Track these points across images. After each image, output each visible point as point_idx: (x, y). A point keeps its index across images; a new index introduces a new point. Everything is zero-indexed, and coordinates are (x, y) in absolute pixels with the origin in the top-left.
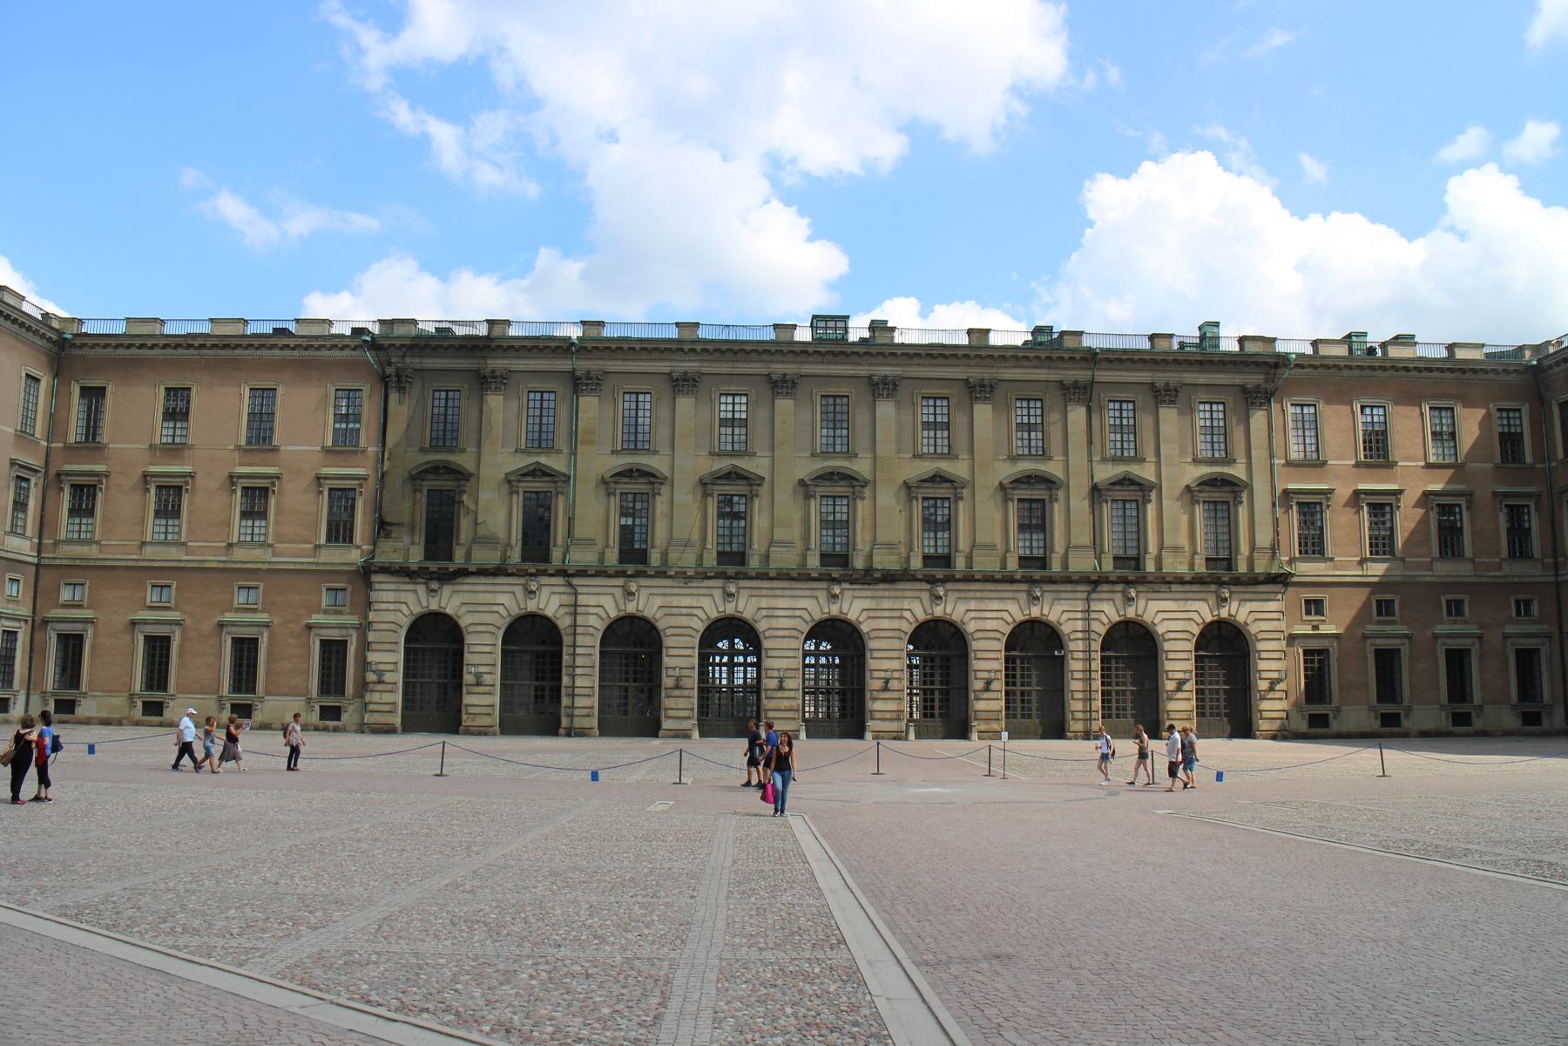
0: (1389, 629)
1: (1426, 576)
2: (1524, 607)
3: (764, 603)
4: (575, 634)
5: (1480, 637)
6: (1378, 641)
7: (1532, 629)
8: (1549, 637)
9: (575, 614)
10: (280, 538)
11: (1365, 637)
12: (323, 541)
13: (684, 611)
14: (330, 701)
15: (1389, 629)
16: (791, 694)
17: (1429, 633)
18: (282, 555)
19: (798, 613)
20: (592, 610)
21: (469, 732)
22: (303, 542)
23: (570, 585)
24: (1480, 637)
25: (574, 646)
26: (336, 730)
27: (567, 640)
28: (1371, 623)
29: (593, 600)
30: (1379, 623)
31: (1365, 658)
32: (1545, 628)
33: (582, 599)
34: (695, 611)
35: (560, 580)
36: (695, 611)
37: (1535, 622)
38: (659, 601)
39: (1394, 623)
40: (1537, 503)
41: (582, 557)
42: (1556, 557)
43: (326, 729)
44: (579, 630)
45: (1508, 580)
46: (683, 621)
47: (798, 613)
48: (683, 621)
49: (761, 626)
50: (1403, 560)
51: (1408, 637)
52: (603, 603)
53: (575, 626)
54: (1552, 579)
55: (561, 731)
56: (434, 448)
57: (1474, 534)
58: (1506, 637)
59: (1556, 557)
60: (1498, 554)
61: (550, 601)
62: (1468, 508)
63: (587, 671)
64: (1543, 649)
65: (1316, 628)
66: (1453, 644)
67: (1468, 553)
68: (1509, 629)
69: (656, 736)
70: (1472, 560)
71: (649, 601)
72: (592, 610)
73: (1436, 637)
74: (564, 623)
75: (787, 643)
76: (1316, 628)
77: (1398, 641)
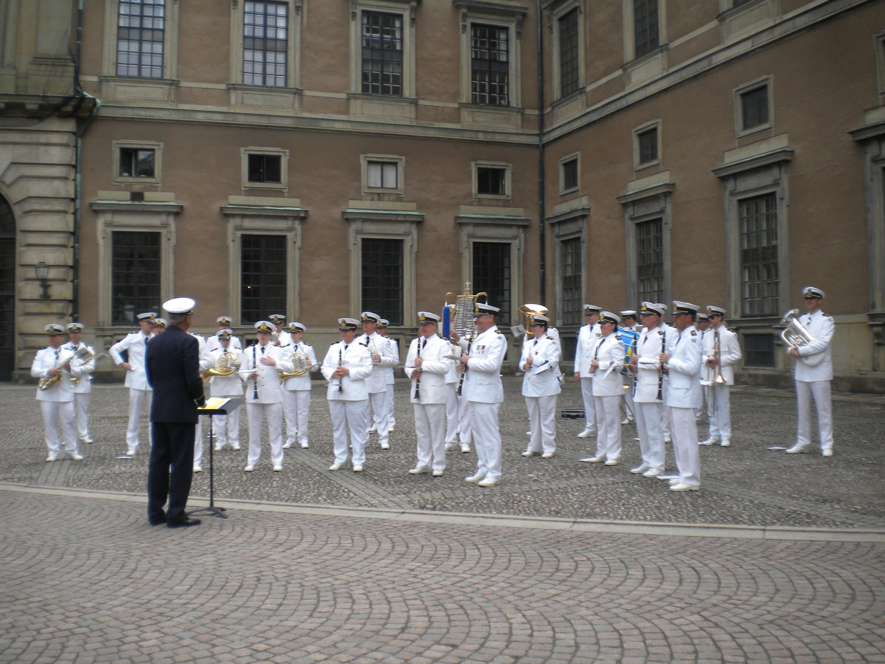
0: (268, 202)
1: (338, 122)
2: (490, 181)
5: (419, 223)
6: (247, 223)
7: (502, 213)
8: (525, 227)
11: (226, 215)
15: (268, 202)
17: (336, 213)
24: (419, 223)
28: (237, 191)
30: (251, 192)
31: (224, 249)
32: (517, 213)
37: (506, 204)
39: (279, 193)
40: (520, 24)
42: (541, 107)
45: (467, 136)
50: (298, 92)
51: (303, 218)
54: (534, 140)
57: (420, 62)
58: (460, 224)
59: (541, 107)
60: (456, 96)
62: (413, 20)
64: (515, 245)
65: (137, 196)
66: (375, 231)
67: (409, 89)
68: (467, 212)
70: (414, 102)
73: (348, 219)
76: (137, 196)
77: (281, 224)
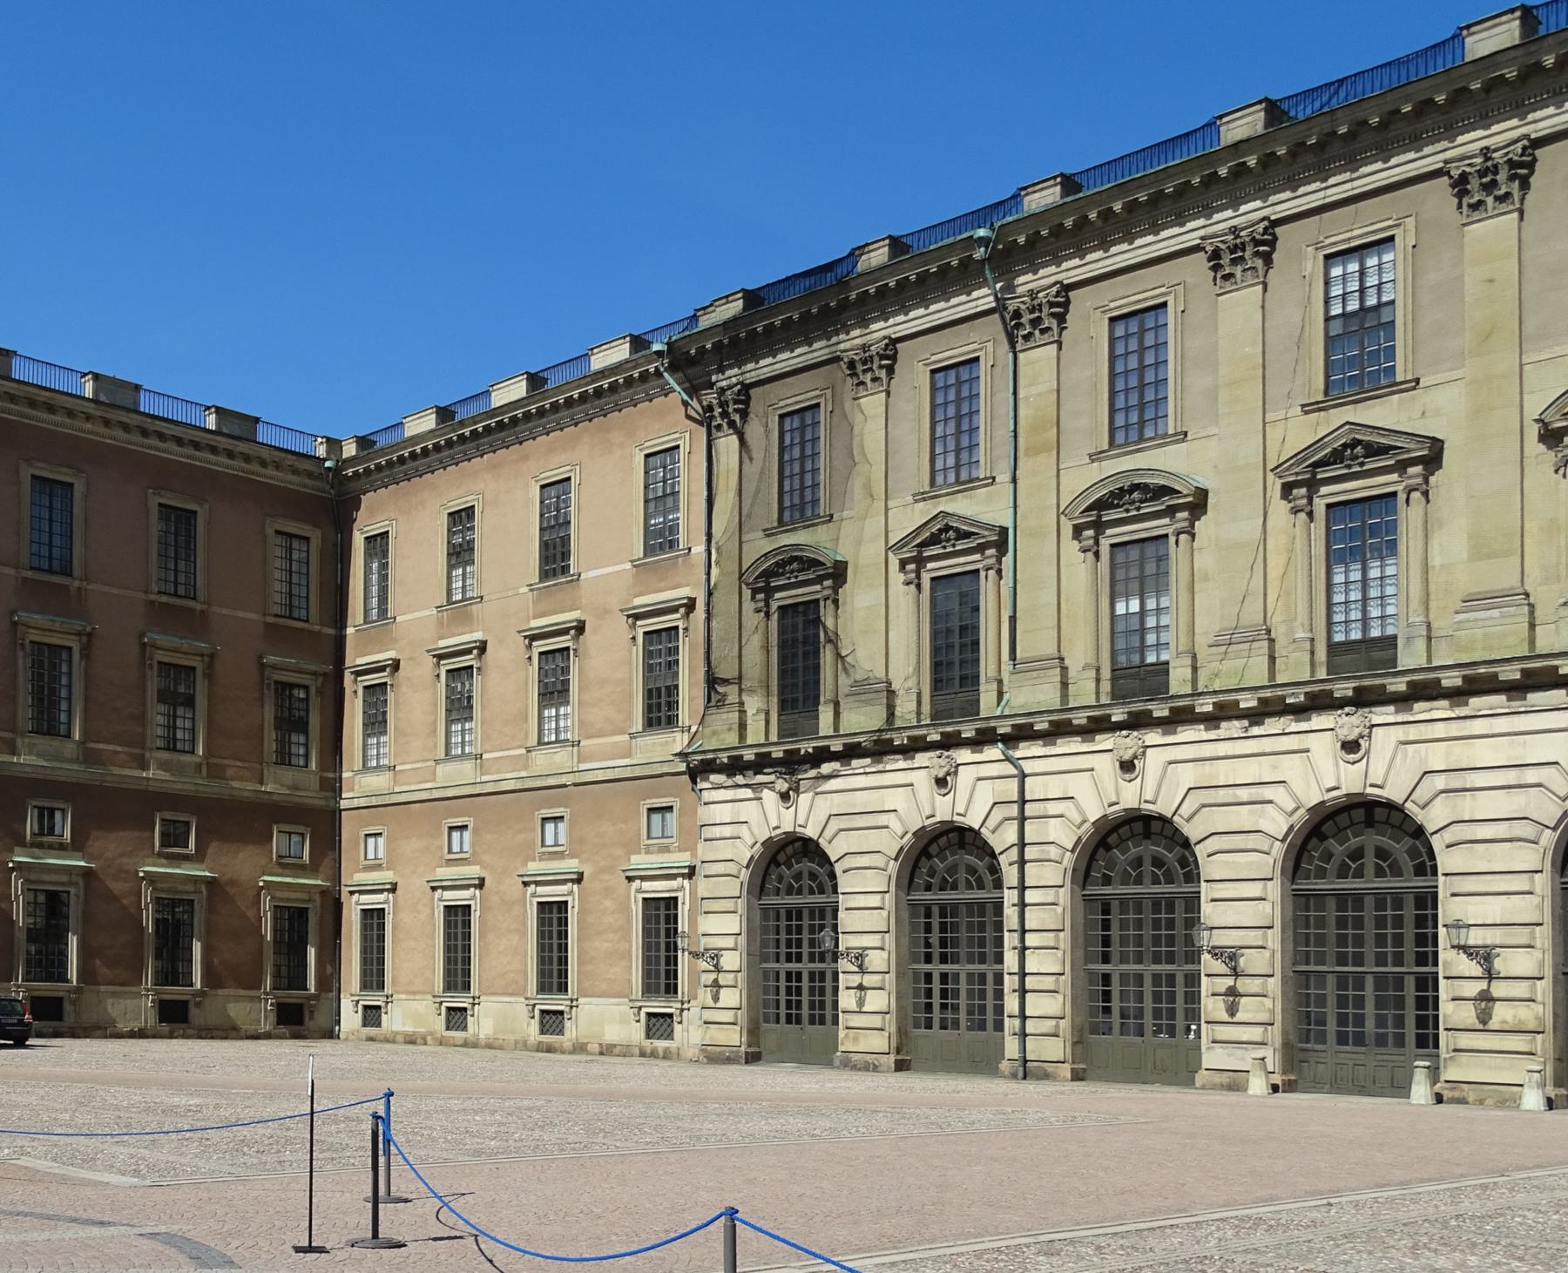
3: (1437, 757)
4: (1022, 862)
9: (1022, 819)
10: (587, 730)
12: (638, 725)
13: (1244, 794)
14: (657, 1006)
16: (1520, 990)
18: (590, 759)
19: (1531, 776)
20: (1053, 808)
21: (848, 1064)
22: (613, 733)
23: (1008, 759)
25: (1022, 888)
26: (667, 1056)
27: (1010, 875)
29: (1054, 787)
33: (1034, 788)
34: (1267, 792)
35: (994, 752)
36: (1267, 792)
38: (1188, 775)
41: (1033, 696)
43: (653, 1054)
44: (1030, 853)
46: (1243, 817)
47: (1531, 776)
48: (1243, 817)
49: (1432, 818)
52: (1080, 786)
53: (1022, 844)
55: (1004, 1066)
56: (783, 523)
61: (976, 791)
63: (1048, 940)
69: (1190, 1083)
71: (1171, 773)
72: (1053, 808)
74: (1002, 839)
75: (1500, 857)
